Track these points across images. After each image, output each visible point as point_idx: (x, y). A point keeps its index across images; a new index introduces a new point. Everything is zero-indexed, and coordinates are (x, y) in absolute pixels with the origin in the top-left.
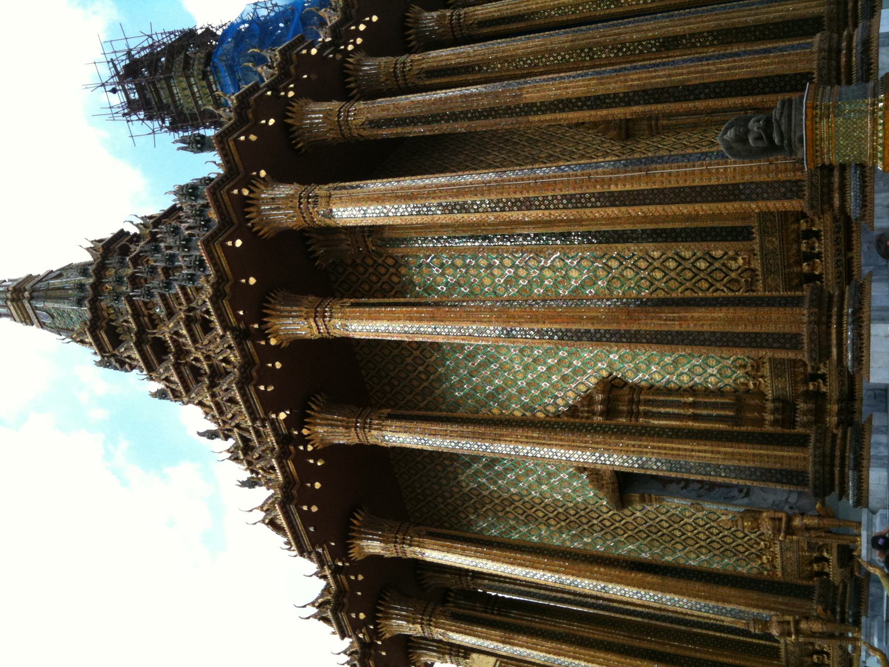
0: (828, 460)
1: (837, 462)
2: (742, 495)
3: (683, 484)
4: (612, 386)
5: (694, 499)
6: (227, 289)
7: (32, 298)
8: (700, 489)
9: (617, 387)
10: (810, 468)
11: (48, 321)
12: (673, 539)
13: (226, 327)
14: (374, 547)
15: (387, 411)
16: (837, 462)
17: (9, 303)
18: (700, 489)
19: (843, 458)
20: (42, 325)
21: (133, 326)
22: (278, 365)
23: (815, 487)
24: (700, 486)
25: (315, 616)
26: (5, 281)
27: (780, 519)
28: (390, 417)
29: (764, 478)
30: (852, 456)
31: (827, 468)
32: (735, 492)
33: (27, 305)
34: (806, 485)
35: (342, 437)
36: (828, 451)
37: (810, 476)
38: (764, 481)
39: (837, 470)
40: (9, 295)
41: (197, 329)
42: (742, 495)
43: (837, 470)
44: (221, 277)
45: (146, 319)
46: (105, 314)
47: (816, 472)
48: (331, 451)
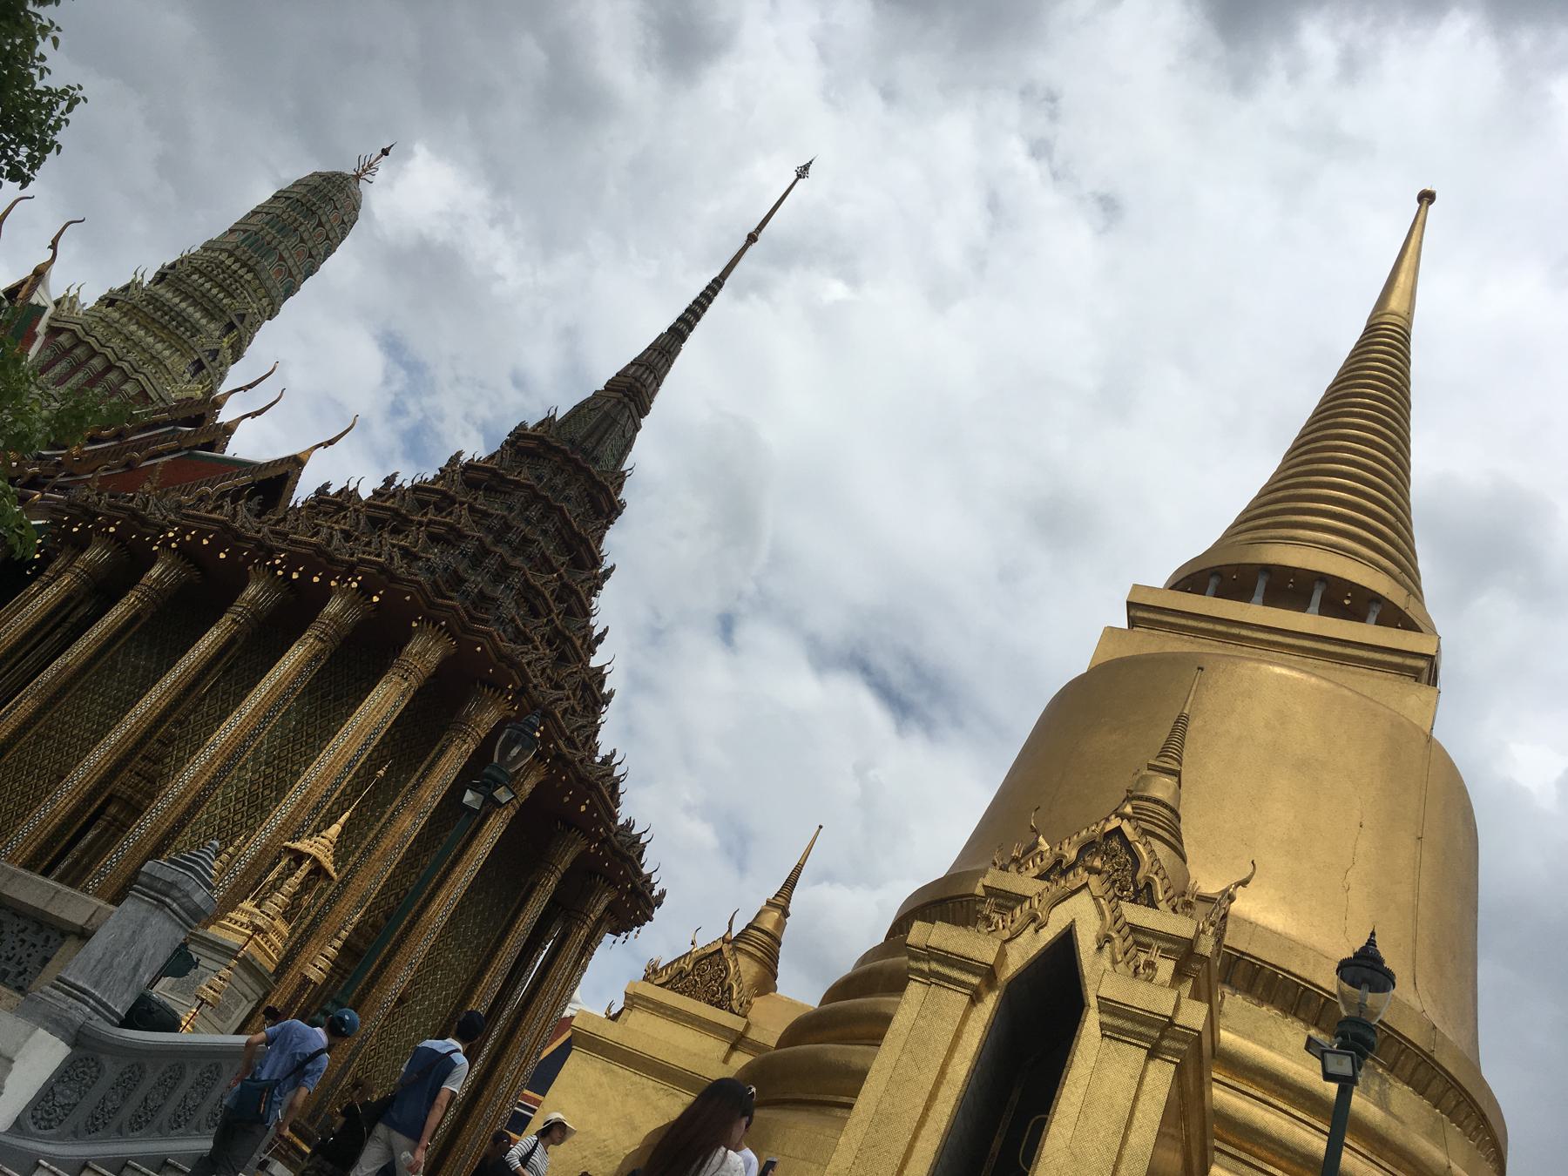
7: (619, 402)
13: (361, 561)
22: (316, 579)
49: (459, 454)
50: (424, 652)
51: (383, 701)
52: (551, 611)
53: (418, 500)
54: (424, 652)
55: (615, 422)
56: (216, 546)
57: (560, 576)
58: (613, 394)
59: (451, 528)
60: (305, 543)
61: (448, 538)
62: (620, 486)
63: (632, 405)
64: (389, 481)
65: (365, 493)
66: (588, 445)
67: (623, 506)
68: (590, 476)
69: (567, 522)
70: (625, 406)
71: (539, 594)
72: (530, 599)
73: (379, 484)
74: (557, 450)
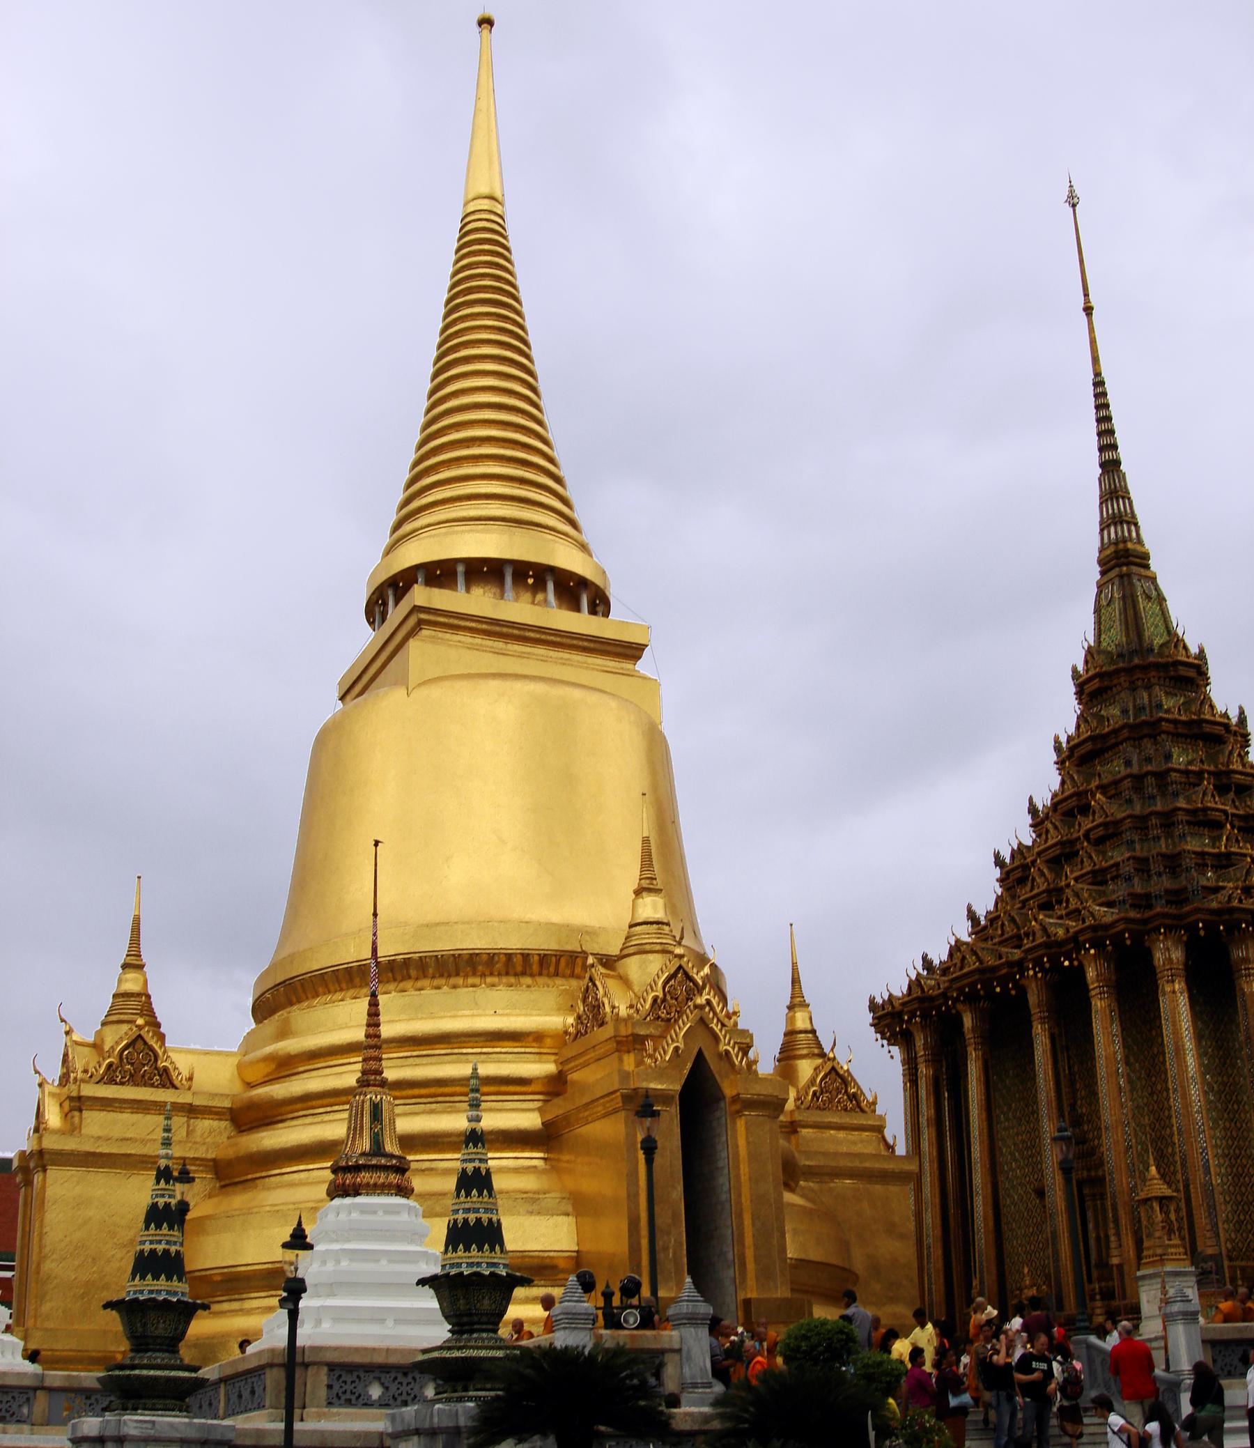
6: (1100, 933)
7: (1121, 576)
11: (1104, 603)
13: (1077, 933)
14: (968, 1021)
15: (1056, 1031)
17: (1112, 549)
20: (1100, 586)
21: (1107, 730)
25: (910, 981)
26: (1136, 524)
28: (1052, 1038)
33: (1116, 571)
35: (1033, 999)
40: (1121, 546)
41: (1101, 832)
44: (1106, 927)
45: (1113, 741)
46: (1115, 682)
48: (1022, 992)
49: (1057, 740)
50: (1168, 954)
51: (1177, 1006)
52: (1225, 812)
53: (1064, 814)
54: (1168, 954)
55: (1134, 598)
56: (988, 986)
57: (1209, 773)
58: (1112, 574)
59: (1105, 825)
60: (1034, 947)
61: (1109, 834)
62: (1185, 647)
63: (1134, 569)
64: (1033, 810)
65: (1028, 838)
66: (1134, 646)
67: (1201, 655)
68: (1157, 666)
69: (1175, 722)
70: (1129, 575)
71: (1205, 810)
72: (1206, 822)
73: (1028, 820)
74: (1117, 672)
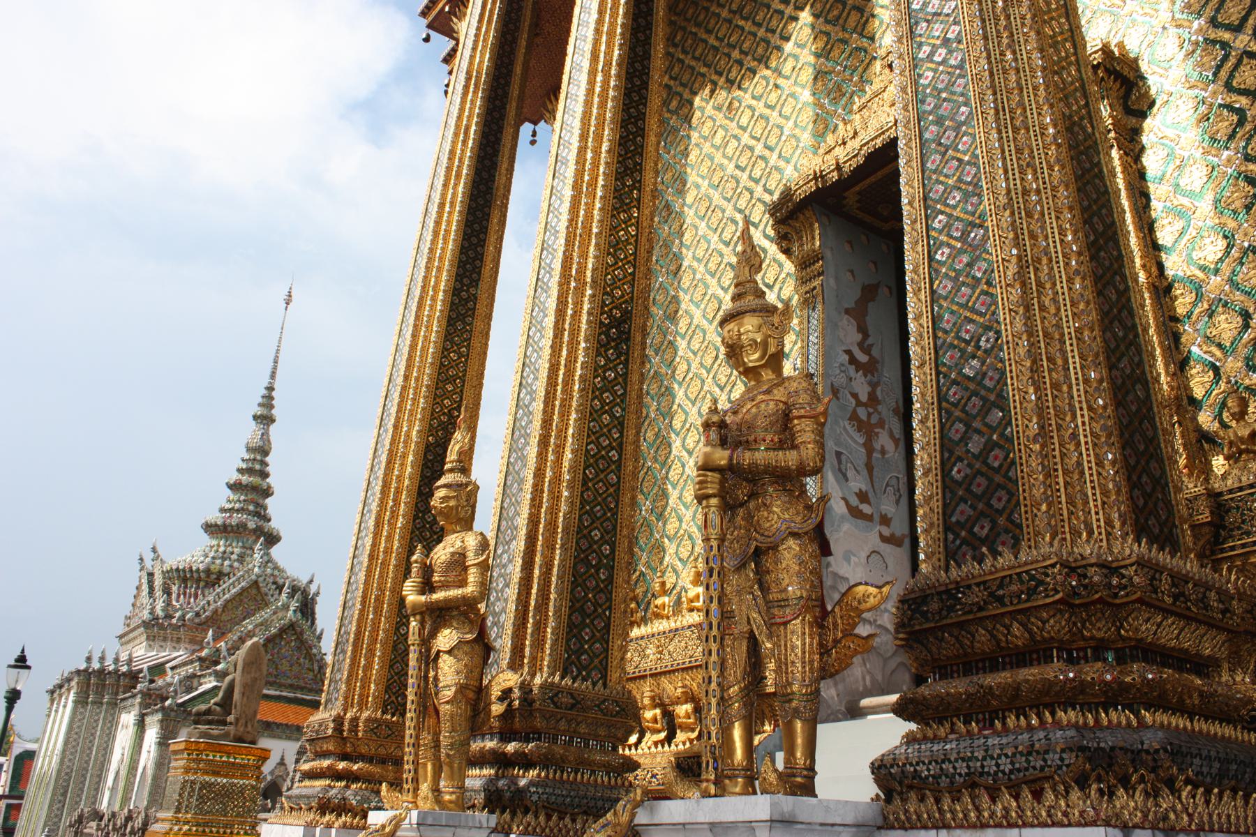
0: (1100, 629)
1: (1100, 672)
2: (854, 501)
3: (862, 358)
4: (1124, 80)
5: (825, 376)
8: (855, 396)
9: (1126, 96)
10: (1041, 551)
12: (722, 389)
16: (1100, 672)
18: (855, 396)
19: (1113, 696)
23: (949, 594)
24: (864, 398)
27: (787, 440)
29: (953, 393)
30: (1152, 740)
31: (1056, 626)
32: (858, 483)
34: (951, 555)
36: (1145, 627)
37: (1005, 559)
38: (941, 397)
39: (1058, 672)
42: (854, 501)
43: (1058, 672)
47: (1034, 582)
